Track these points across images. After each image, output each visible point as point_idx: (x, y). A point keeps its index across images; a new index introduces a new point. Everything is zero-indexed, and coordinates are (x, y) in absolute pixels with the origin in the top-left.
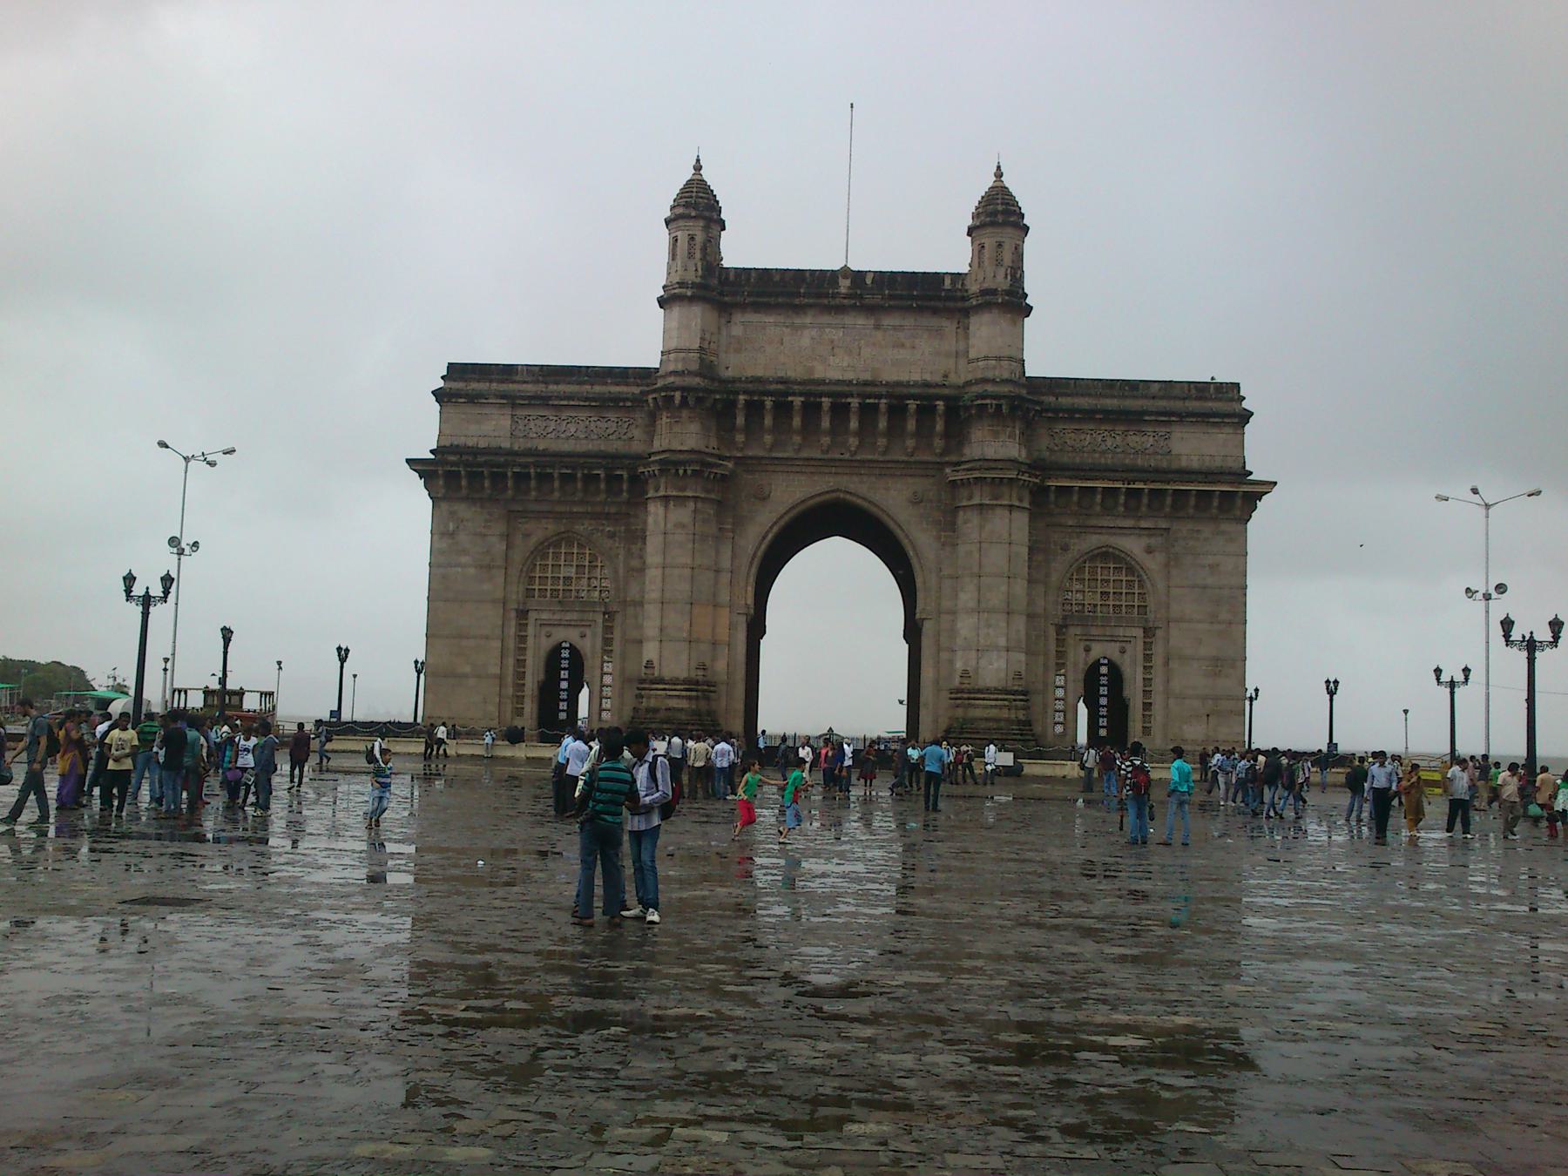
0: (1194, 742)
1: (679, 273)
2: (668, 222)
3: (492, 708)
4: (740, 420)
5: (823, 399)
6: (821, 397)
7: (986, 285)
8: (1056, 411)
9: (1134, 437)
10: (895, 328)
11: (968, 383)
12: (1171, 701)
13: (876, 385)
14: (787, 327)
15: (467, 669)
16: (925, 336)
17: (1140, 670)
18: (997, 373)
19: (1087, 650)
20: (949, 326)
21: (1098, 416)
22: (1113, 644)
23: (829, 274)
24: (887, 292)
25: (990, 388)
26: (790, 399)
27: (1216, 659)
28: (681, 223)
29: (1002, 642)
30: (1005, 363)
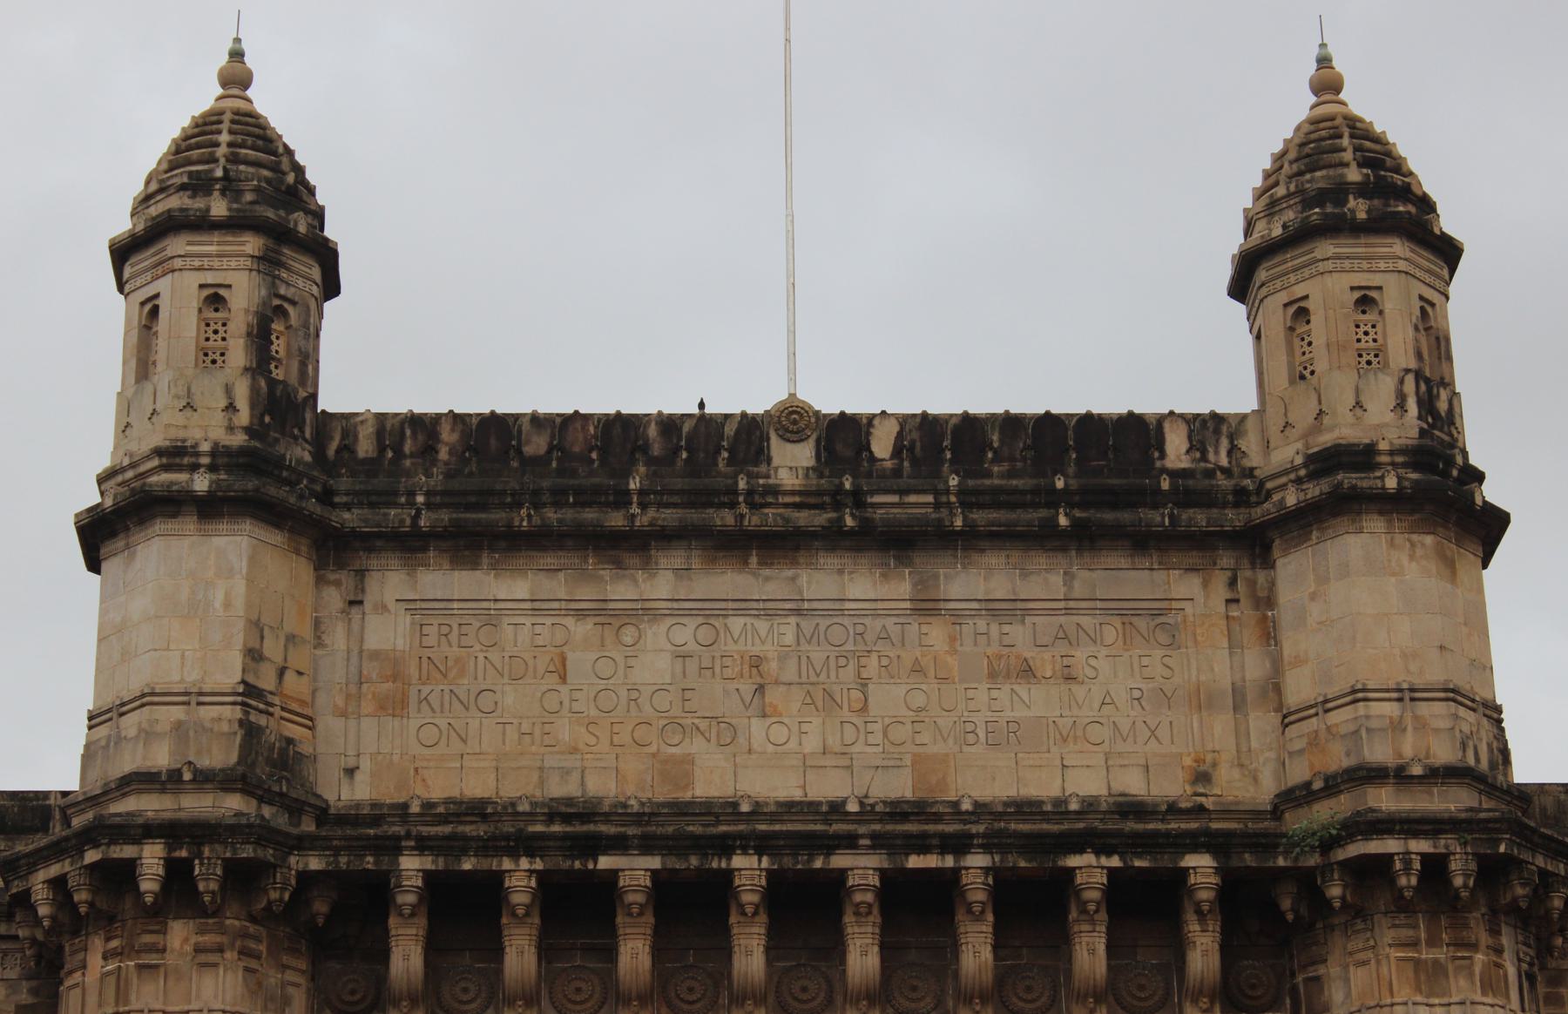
1: (165, 418)
2: (122, 252)
5: (738, 861)
7: (1326, 439)
10: (994, 609)
11: (1295, 797)
13: (937, 818)
14: (581, 614)
16: (1110, 634)
18: (1408, 751)
23: (730, 430)
24: (954, 481)
25: (1384, 800)
26: (605, 862)
28: (177, 245)
30: (1436, 713)
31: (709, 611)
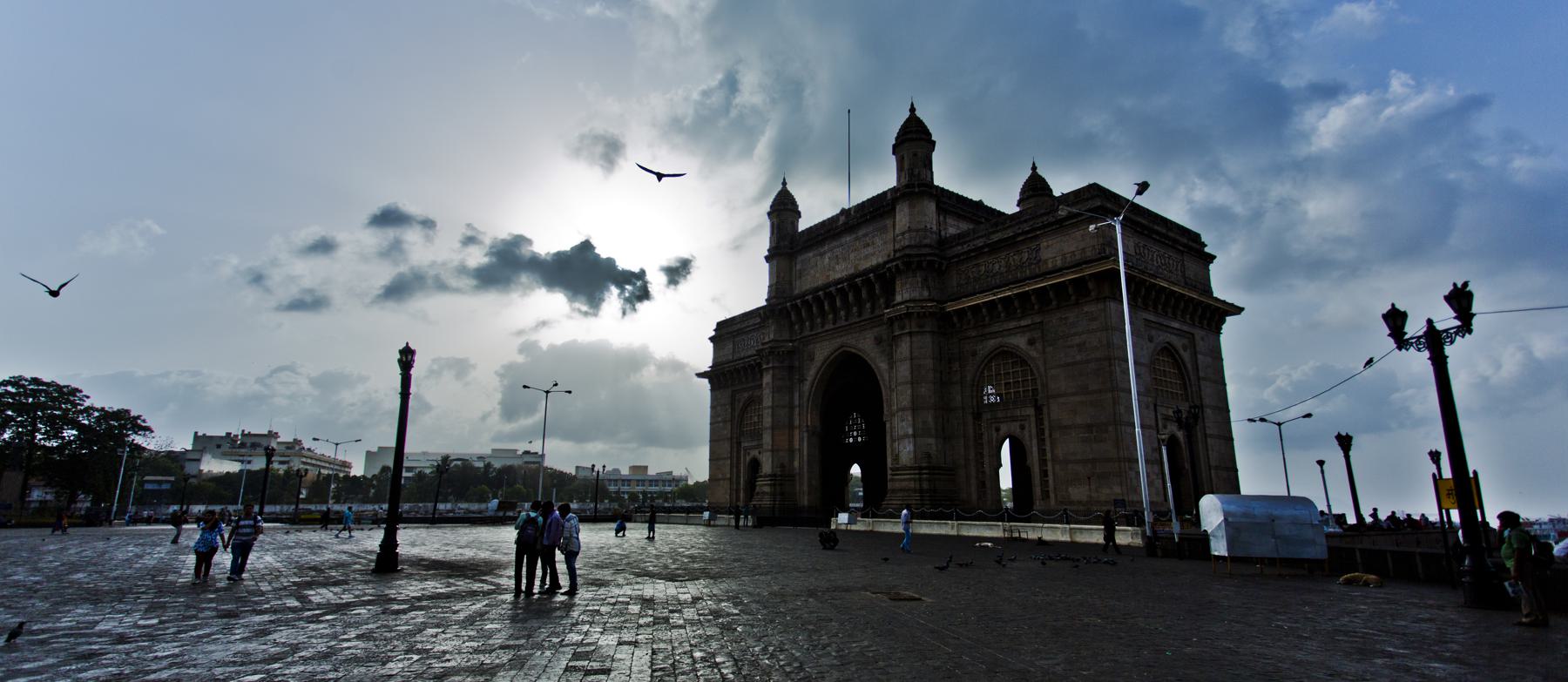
0: (1080, 502)
3: (728, 497)
4: (793, 317)
6: (818, 291)
8: (958, 256)
9: (1016, 257)
10: (865, 235)
12: (1057, 467)
15: (720, 476)
17: (1035, 441)
19: (998, 430)
20: (889, 222)
21: (986, 250)
22: (1015, 423)
26: (807, 298)
27: (1089, 427)
29: (910, 431)
30: (907, 235)
31: (831, 250)
